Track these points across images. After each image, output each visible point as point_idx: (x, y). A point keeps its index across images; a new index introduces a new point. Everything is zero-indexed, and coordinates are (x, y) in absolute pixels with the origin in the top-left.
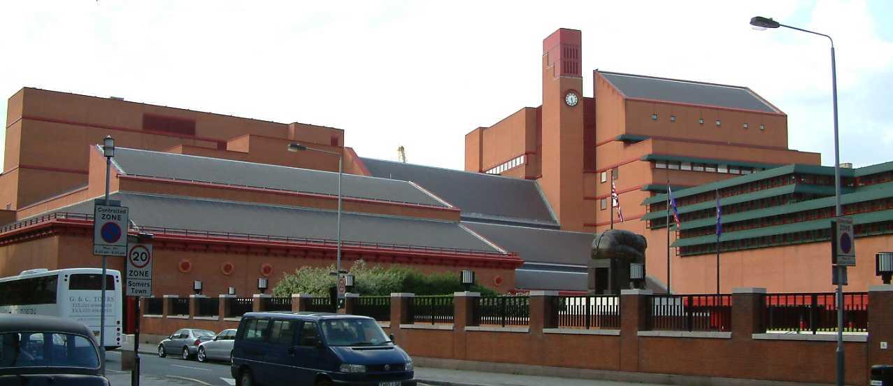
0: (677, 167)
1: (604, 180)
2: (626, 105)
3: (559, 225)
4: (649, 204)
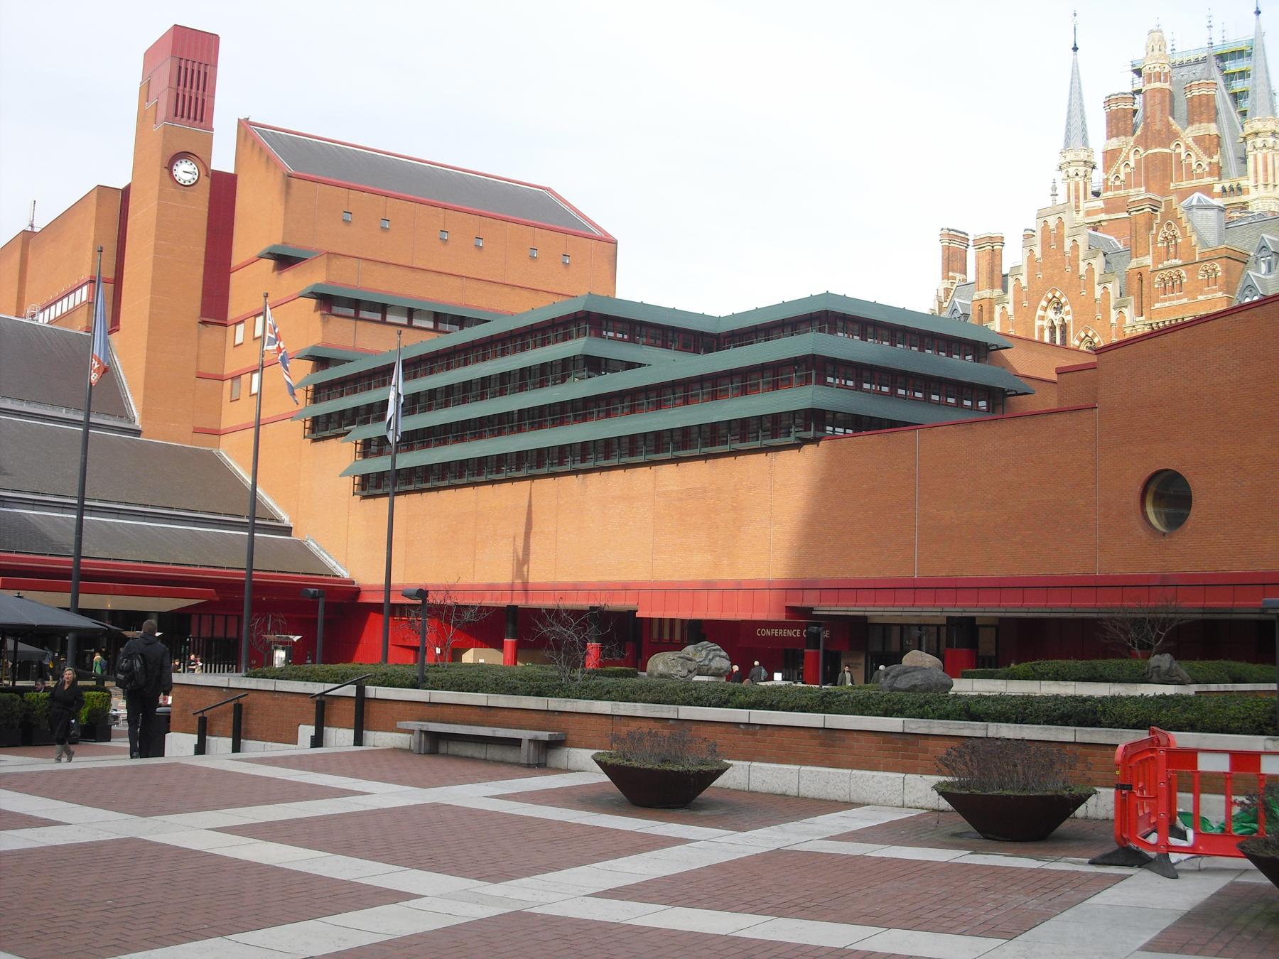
0: (378, 317)
1: (239, 340)
2: (288, 186)
3: (138, 424)
4: (311, 387)
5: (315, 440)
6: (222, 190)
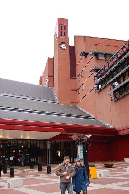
5: (99, 92)
6: (72, 50)
